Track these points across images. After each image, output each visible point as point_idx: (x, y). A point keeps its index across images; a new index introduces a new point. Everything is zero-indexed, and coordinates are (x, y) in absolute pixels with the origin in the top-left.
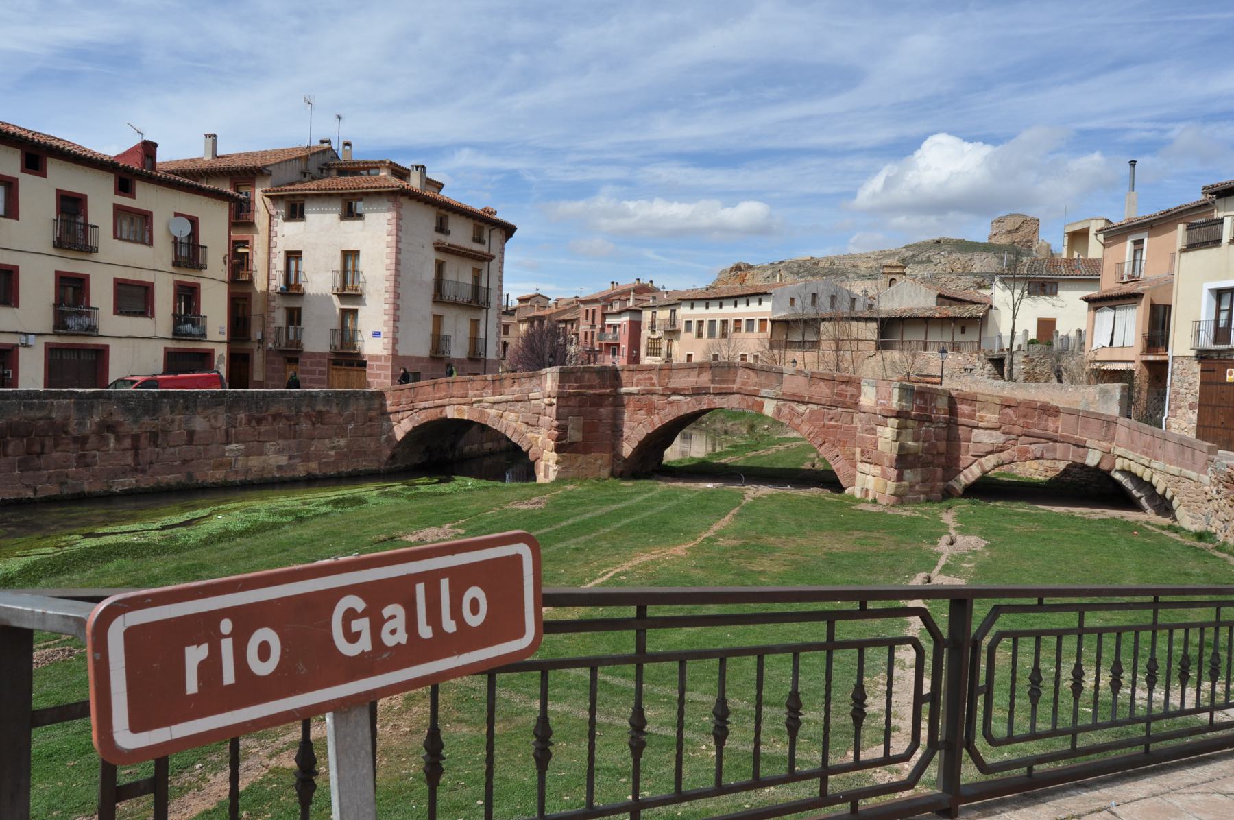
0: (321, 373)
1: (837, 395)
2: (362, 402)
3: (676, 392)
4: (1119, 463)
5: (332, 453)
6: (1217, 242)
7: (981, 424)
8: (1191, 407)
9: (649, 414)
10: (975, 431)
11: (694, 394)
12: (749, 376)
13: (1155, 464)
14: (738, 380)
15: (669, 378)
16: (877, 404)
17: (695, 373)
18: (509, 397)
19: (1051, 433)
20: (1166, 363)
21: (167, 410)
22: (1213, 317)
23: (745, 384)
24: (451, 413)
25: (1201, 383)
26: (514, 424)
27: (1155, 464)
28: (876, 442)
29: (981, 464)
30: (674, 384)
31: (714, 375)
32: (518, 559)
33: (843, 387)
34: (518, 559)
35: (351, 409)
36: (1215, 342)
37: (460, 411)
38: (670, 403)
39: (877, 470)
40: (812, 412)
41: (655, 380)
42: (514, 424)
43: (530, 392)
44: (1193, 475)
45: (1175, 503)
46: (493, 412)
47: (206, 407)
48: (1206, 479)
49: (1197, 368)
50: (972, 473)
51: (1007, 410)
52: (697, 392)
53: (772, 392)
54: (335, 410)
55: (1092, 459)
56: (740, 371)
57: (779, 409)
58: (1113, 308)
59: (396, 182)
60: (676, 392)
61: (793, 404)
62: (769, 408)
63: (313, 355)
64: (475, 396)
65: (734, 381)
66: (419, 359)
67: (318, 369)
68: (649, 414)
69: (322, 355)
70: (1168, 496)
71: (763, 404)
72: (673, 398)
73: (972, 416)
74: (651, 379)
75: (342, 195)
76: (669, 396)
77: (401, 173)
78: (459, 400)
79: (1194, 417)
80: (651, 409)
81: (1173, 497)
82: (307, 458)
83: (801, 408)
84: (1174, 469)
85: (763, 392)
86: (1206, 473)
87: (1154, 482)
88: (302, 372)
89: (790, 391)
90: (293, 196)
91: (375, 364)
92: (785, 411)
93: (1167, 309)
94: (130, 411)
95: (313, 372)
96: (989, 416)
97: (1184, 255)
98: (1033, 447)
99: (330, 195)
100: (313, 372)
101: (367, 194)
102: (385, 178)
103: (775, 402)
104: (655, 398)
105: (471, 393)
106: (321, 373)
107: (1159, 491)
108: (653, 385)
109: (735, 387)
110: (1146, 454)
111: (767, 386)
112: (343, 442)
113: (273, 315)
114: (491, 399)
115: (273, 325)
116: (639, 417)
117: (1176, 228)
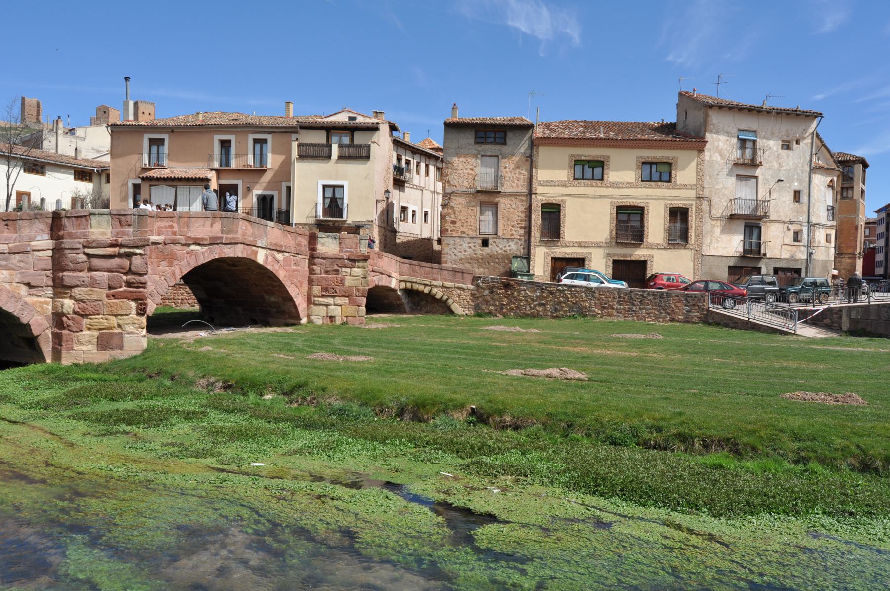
4: (403, 285)
6: (329, 157)
9: (170, 264)
11: (209, 244)
14: (240, 231)
15: (188, 226)
16: (341, 251)
17: (208, 223)
23: (244, 235)
26: (7, 286)
27: (434, 283)
28: (342, 281)
30: (193, 234)
33: (299, 238)
36: (325, 215)
38: (188, 253)
39: (346, 300)
41: (176, 228)
42: (7, 286)
43: (32, 239)
44: (464, 286)
45: (450, 301)
52: (214, 242)
55: (393, 284)
57: (266, 256)
58: (175, 187)
61: (275, 253)
68: (170, 264)
71: (256, 253)
72: (193, 247)
74: (172, 227)
76: (189, 245)
80: (171, 259)
83: (280, 256)
89: (274, 241)
92: (270, 259)
98: (375, 278)
104: (178, 247)
108: (174, 233)
109: (239, 236)
110: (427, 278)
116: (160, 268)
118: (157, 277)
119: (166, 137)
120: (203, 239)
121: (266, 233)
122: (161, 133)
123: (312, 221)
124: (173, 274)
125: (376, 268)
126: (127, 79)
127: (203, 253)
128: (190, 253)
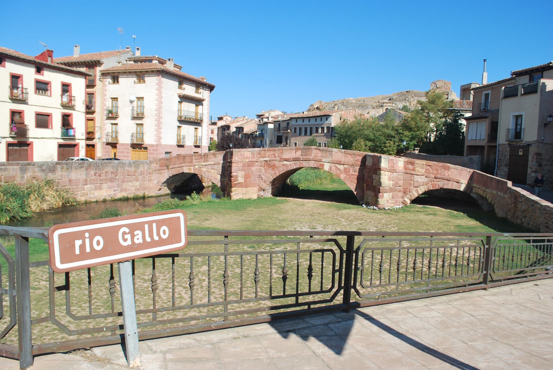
0: (127, 153)
1: (356, 161)
2: (146, 166)
3: (286, 160)
5: (133, 188)
7: (417, 173)
8: (506, 165)
9: (273, 169)
10: (415, 176)
12: (317, 153)
13: (487, 190)
15: (282, 153)
17: (294, 151)
18: (212, 163)
19: (446, 177)
20: (496, 146)
21: (59, 170)
22: (514, 128)
24: (186, 170)
25: (510, 156)
28: (373, 182)
29: (417, 190)
31: (302, 152)
32: (179, 218)
34: (179, 218)
35: (141, 169)
37: (190, 169)
38: (282, 165)
40: (345, 169)
41: (277, 155)
45: (495, 206)
46: (204, 169)
47: (76, 169)
48: (506, 196)
49: (508, 149)
50: (413, 194)
51: (429, 167)
52: (296, 160)
53: (328, 160)
54: (133, 169)
56: (314, 151)
57: (331, 168)
59: (160, 67)
60: (286, 160)
62: (327, 167)
63: (123, 144)
64: (196, 162)
65: (311, 155)
66: (171, 146)
67: (126, 151)
68: (273, 169)
69: (127, 144)
70: (493, 203)
71: (323, 165)
72: (285, 162)
73: (414, 170)
75: (136, 72)
77: (162, 62)
78: (190, 164)
79: (507, 170)
80: (273, 167)
81: (494, 204)
82: (122, 191)
83: (341, 167)
84: (494, 192)
85: (324, 160)
86: (507, 194)
87: (487, 198)
88: (119, 152)
90: (114, 73)
91: (152, 148)
92: (333, 168)
93: (497, 123)
94: (43, 171)
95: (123, 152)
96: (420, 170)
97: (503, 100)
99: (130, 72)
100: (123, 152)
101: (147, 72)
102: (155, 64)
103: (329, 164)
105: (194, 161)
106: (127, 153)
107: (490, 201)
108: (275, 157)
109: (311, 158)
110: (485, 186)
111: (326, 157)
112: (137, 184)
113: (105, 127)
114: (204, 164)
115: (105, 131)
117: (458, 97)
118: (267, 175)
119: (489, 92)
120: (289, 159)
121: (331, 155)
122: (489, 90)
123: (507, 143)
124: (275, 173)
125: (439, 176)
126: (485, 60)
127: (291, 165)
128: (284, 165)
